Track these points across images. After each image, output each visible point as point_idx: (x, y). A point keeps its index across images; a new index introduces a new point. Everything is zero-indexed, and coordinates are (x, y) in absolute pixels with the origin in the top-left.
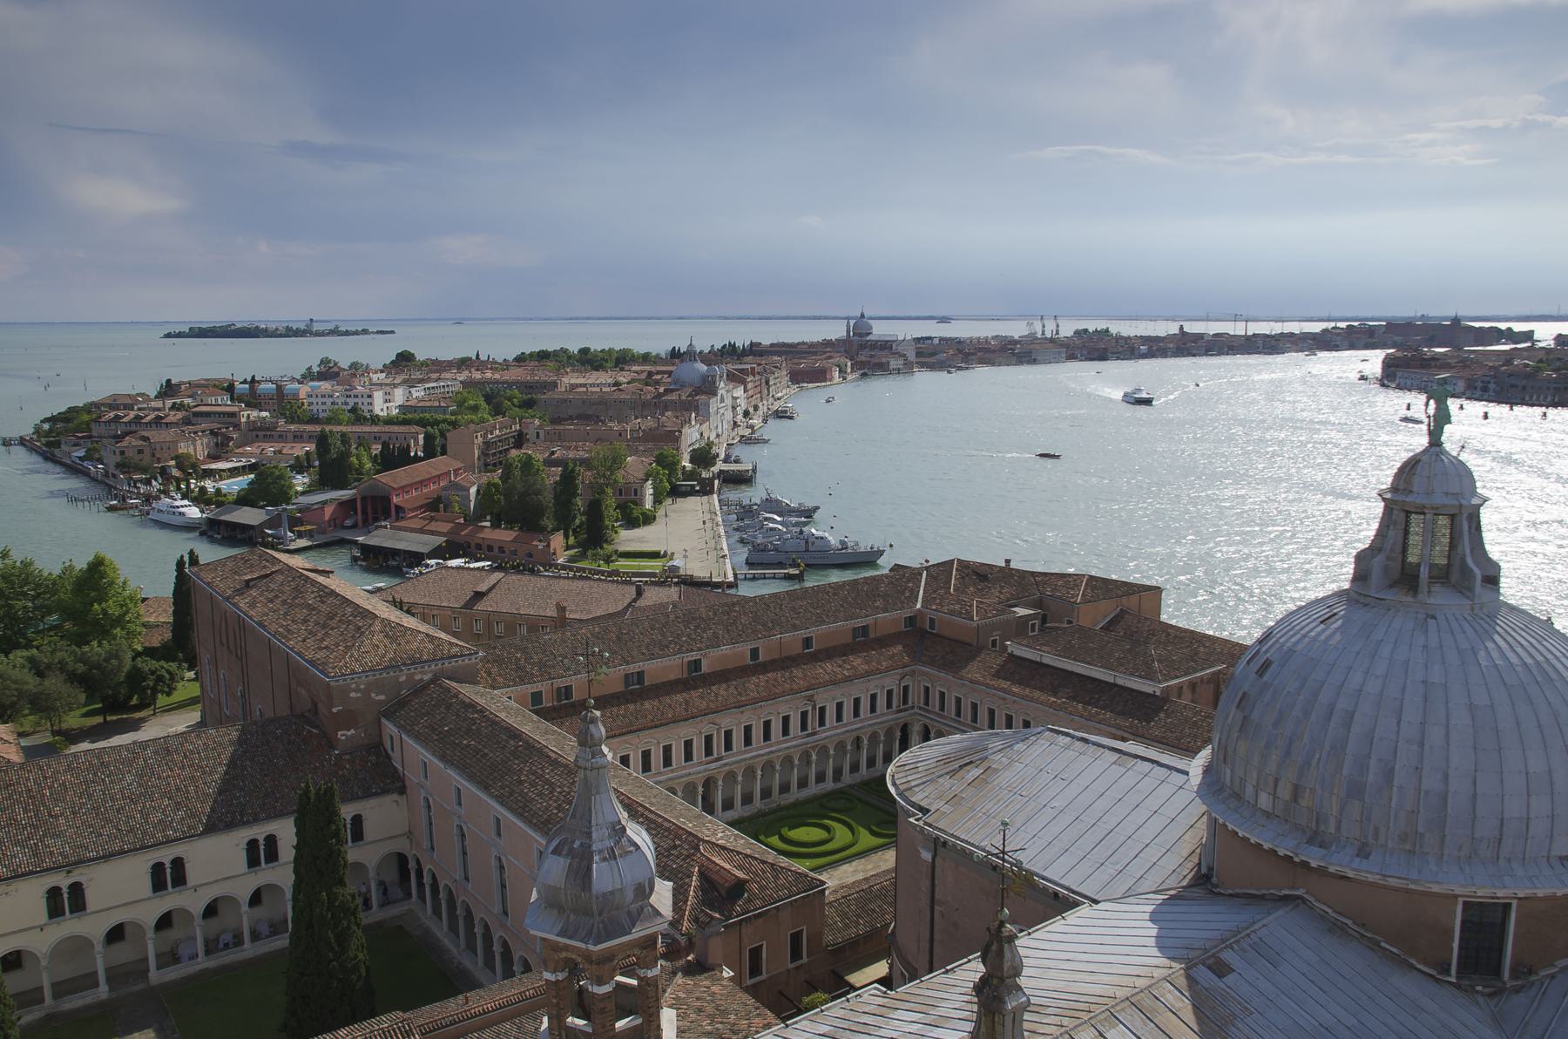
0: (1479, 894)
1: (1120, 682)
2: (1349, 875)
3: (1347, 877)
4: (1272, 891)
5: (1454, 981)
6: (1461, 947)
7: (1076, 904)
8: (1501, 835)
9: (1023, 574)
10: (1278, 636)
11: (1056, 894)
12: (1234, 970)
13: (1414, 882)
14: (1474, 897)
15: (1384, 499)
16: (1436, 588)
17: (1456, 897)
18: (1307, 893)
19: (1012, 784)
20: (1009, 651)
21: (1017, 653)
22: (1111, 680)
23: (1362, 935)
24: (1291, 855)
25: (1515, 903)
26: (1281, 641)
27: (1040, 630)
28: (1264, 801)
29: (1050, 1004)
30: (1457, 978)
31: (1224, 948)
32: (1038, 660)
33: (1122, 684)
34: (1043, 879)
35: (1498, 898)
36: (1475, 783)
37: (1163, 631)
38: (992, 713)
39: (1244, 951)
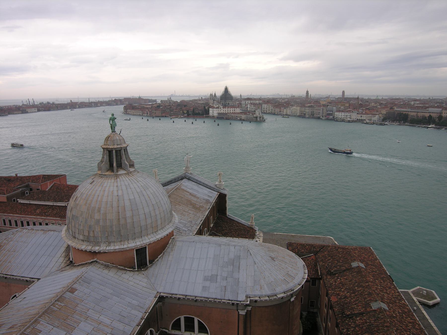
0: (138, 247)
1: (55, 204)
2: (106, 252)
3: (106, 252)
4: (88, 261)
5: (137, 270)
6: (137, 261)
7: (34, 281)
8: (141, 231)
9: (22, 177)
10: (79, 189)
11: (27, 281)
12: (77, 290)
13: (123, 249)
14: (137, 248)
15: (102, 148)
16: (119, 169)
17: (134, 249)
18: (97, 259)
19: (9, 249)
20: (19, 202)
21: (22, 202)
22: (52, 204)
23: (113, 266)
24: (91, 250)
25: (147, 246)
26: (80, 191)
27: (30, 193)
28: (81, 237)
29: (18, 323)
30: (137, 269)
31: (74, 284)
32: (29, 203)
33: (56, 205)
34: (22, 277)
35: (143, 246)
36: (133, 219)
37: (67, 187)
38: (16, 222)
39: (80, 283)
